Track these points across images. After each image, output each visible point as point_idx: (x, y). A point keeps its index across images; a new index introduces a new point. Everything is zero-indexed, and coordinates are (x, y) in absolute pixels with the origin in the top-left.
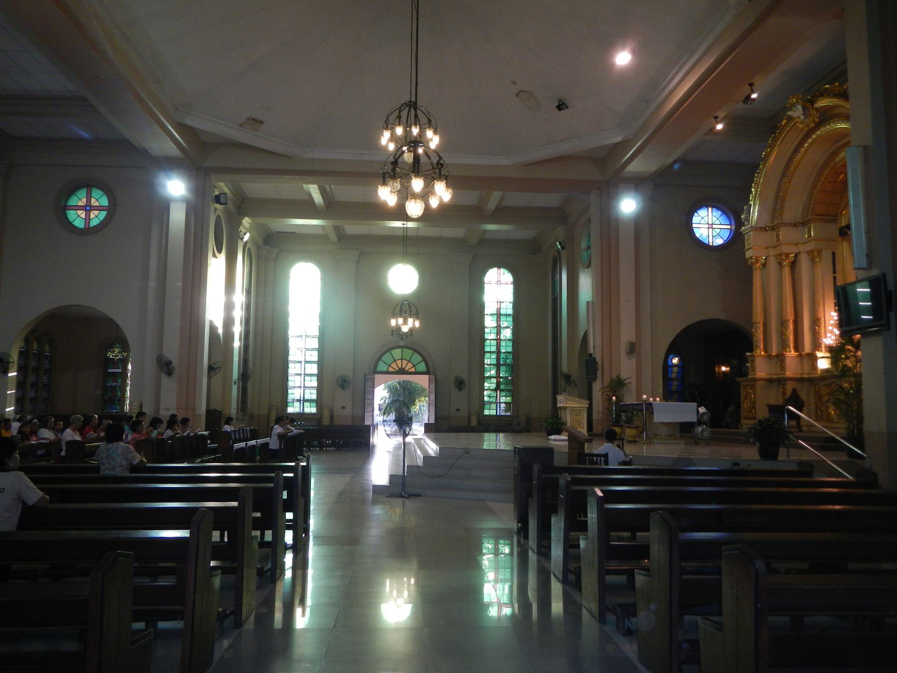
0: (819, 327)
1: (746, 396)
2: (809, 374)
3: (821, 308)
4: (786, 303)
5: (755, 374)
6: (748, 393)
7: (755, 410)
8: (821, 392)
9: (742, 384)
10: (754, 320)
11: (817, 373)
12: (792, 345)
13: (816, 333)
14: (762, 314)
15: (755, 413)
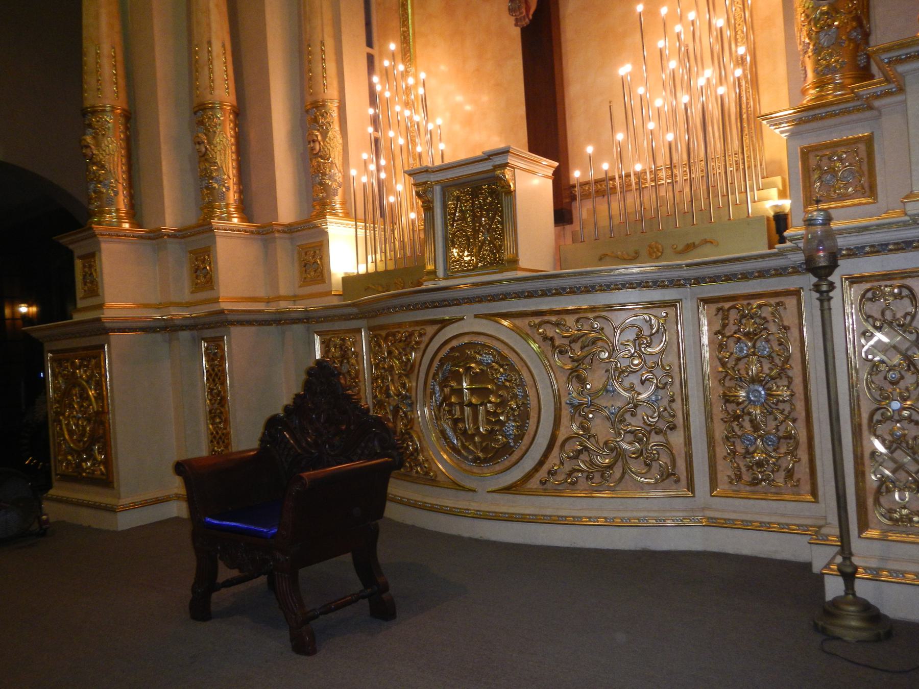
0: (325, 135)
1: (67, 394)
2: (295, 298)
3: (331, 67)
4: (209, 43)
5: (100, 307)
6: (73, 382)
7: (106, 448)
8: (353, 361)
9: (47, 346)
10: (90, 99)
11: (328, 293)
12: (232, 197)
13: (317, 155)
14: (121, 82)
15: (107, 463)
